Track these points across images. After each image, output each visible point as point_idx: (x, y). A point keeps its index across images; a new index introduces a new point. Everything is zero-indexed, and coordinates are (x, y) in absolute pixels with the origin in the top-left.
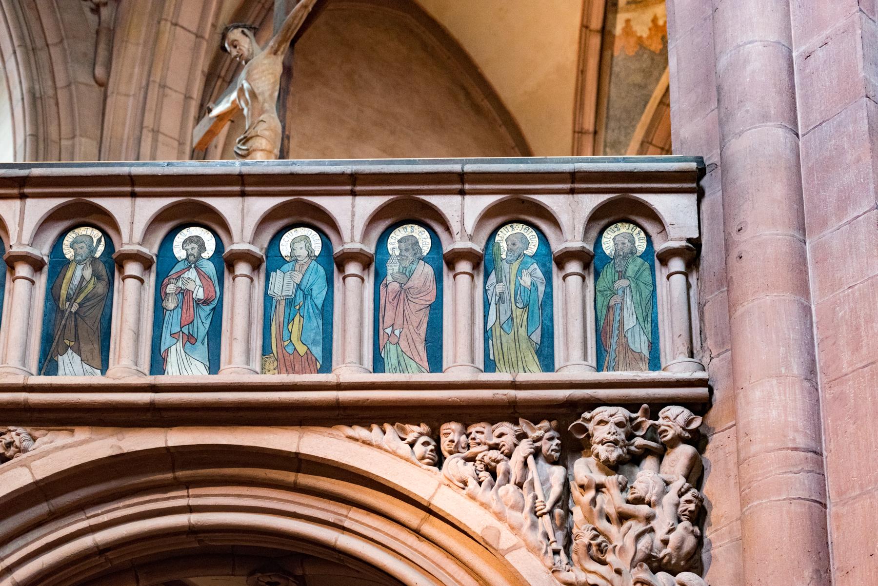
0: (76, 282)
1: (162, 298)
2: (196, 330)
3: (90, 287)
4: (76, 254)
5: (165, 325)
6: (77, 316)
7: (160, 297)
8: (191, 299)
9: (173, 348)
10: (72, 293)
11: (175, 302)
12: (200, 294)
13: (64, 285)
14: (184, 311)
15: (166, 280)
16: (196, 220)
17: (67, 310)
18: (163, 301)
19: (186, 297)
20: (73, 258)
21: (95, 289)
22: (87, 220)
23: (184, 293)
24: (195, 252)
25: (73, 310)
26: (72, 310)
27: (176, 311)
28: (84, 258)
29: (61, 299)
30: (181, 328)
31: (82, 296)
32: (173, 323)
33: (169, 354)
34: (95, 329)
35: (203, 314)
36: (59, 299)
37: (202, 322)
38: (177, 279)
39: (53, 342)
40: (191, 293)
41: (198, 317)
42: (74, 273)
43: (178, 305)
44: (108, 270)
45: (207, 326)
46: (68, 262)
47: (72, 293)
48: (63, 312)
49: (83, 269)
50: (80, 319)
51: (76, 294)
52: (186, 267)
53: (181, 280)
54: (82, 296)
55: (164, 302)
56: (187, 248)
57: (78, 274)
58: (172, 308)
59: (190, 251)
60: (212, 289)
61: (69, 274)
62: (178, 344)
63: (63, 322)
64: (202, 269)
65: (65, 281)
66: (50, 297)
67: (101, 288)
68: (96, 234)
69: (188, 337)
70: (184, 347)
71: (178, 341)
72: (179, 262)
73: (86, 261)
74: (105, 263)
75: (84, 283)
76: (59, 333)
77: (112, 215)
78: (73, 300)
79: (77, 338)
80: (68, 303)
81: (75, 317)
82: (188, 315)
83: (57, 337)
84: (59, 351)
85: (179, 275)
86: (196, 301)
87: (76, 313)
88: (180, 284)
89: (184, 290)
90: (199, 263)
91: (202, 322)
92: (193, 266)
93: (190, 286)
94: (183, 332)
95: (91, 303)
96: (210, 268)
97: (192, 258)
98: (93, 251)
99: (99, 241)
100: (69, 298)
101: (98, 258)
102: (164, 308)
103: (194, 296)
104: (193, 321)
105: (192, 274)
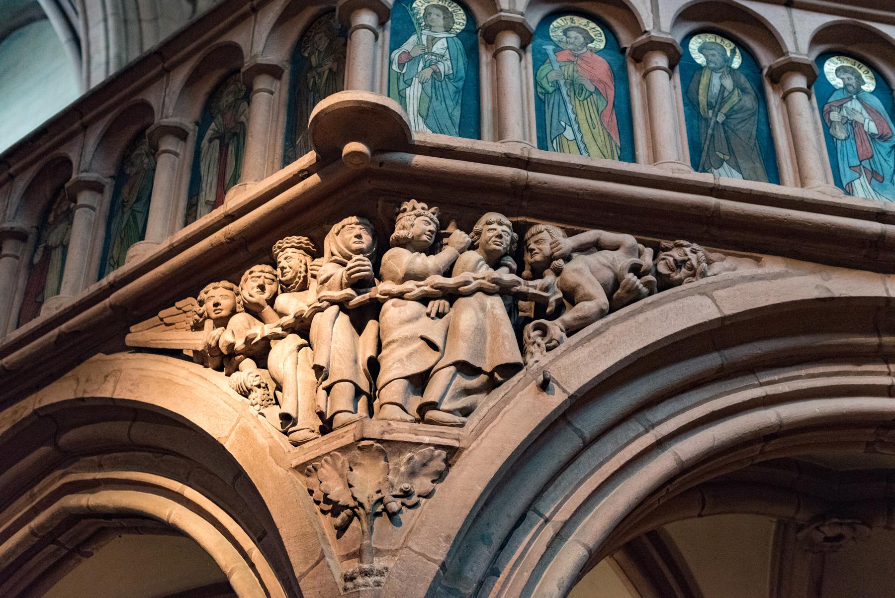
0: (716, 89)
1: (827, 126)
2: (879, 167)
3: (735, 98)
4: (708, 62)
5: (839, 155)
6: (726, 128)
7: (827, 125)
8: (863, 132)
9: (857, 183)
10: (713, 101)
11: (844, 132)
12: (872, 127)
13: (701, 91)
14: (859, 143)
15: (827, 107)
16: (850, 48)
17: (711, 119)
18: (829, 128)
19: (856, 129)
20: (704, 64)
21: (742, 102)
22: (718, 26)
23: (853, 125)
24: (853, 81)
25: (721, 118)
26: (718, 120)
27: (848, 142)
28: (719, 66)
29: (701, 106)
30: (861, 162)
31: (725, 109)
32: (849, 156)
33: (854, 189)
34: (752, 145)
35: (883, 152)
36: (699, 105)
37: (885, 160)
38: (841, 107)
39: (701, 153)
40: (861, 126)
41: (878, 152)
42: (710, 80)
43: (849, 136)
44: (753, 84)
45: (892, 164)
46: (700, 68)
47: (713, 101)
48: (707, 120)
49: (720, 78)
50: (730, 131)
51: (718, 103)
52: (846, 96)
53: (844, 110)
54: (725, 109)
55: (831, 129)
56: (842, 76)
57: (716, 81)
58: (843, 138)
59: (847, 81)
60: (885, 125)
61: (704, 80)
62: (861, 178)
63: (710, 131)
64: (868, 102)
65: (701, 87)
66: (687, 101)
67: (749, 101)
68: (728, 46)
69: (872, 173)
70: (870, 184)
71: (860, 175)
72: (836, 90)
73: (722, 70)
74: (747, 76)
75: (726, 94)
76: (707, 143)
77: (766, 21)
78: (716, 109)
79: (731, 152)
80: (711, 112)
81: (724, 129)
82: (864, 148)
83: (706, 148)
84: (713, 163)
85: (841, 103)
86: (869, 135)
87: (723, 124)
88: (844, 113)
89: (852, 121)
90: (860, 95)
91: (885, 160)
92: (854, 97)
93: (858, 118)
94: (864, 167)
95: (739, 115)
96: (876, 102)
97: (851, 89)
98: (729, 61)
99: (733, 52)
100: (710, 106)
101: (737, 69)
102: (833, 137)
103: (866, 129)
104: (872, 157)
105: (855, 105)
